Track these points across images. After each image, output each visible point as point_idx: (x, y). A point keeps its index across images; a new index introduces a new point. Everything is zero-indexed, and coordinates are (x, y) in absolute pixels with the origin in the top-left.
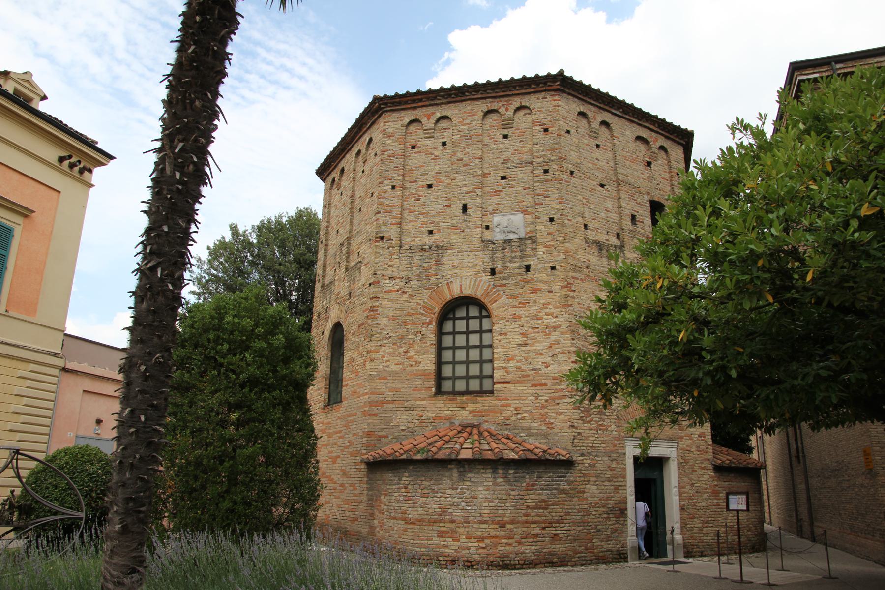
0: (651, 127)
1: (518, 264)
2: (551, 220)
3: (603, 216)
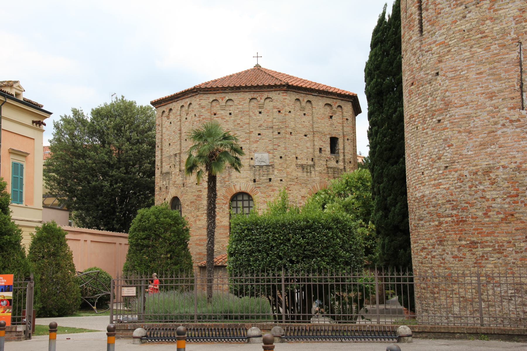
0: (334, 97)
1: (265, 178)
2: (281, 157)
3: (305, 151)
